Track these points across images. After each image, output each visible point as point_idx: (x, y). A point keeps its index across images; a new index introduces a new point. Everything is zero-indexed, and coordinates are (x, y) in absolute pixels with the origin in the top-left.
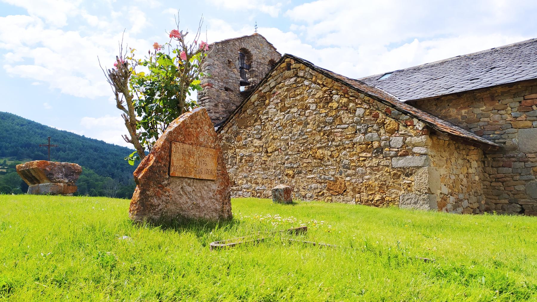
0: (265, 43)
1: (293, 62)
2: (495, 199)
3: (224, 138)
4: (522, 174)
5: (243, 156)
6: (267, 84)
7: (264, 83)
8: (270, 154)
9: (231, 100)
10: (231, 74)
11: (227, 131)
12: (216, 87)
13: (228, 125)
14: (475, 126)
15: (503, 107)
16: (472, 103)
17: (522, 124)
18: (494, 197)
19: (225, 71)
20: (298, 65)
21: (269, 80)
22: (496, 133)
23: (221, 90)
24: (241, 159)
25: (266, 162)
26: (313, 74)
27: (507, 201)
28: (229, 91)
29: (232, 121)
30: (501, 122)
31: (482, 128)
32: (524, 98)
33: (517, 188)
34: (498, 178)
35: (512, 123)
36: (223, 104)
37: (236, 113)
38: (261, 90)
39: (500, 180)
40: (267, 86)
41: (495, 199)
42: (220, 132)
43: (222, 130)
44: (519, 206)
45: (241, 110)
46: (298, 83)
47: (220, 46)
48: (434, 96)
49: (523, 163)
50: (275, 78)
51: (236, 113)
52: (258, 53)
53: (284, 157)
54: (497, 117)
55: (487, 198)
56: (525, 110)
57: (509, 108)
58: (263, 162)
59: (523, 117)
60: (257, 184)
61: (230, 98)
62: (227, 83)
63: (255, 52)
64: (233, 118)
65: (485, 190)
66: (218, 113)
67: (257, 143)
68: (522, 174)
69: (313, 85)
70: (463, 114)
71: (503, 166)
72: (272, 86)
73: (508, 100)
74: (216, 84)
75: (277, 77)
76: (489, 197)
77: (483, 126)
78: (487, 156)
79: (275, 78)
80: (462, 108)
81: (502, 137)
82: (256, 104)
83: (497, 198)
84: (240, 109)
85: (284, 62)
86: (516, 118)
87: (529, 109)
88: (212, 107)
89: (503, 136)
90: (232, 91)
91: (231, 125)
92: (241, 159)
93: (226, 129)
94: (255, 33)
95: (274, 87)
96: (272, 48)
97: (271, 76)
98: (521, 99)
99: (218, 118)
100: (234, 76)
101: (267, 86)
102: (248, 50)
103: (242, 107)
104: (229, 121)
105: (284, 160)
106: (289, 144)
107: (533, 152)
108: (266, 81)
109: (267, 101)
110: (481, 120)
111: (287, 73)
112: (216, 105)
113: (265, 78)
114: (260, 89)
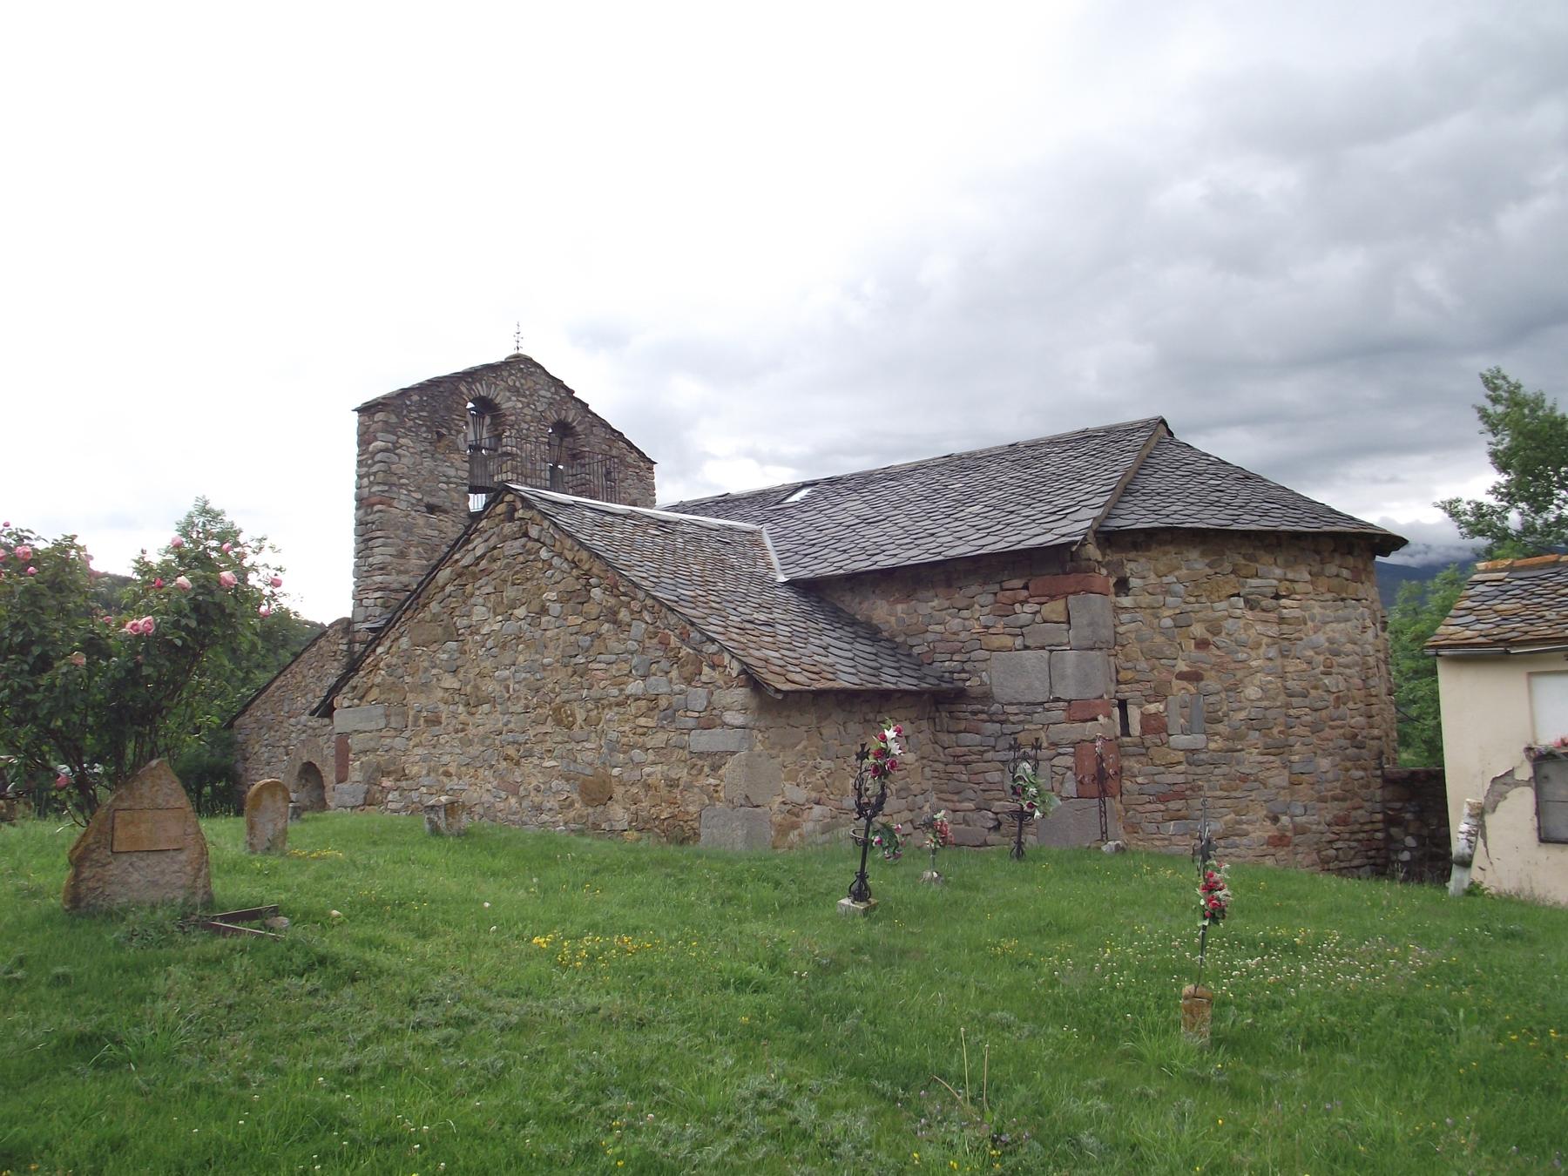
0: (542, 380)
1: (519, 505)
2: (952, 801)
3: (381, 665)
4: (997, 749)
5: (420, 711)
6: (470, 547)
7: (462, 546)
8: (474, 710)
9: (443, 535)
10: (446, 469)
11: (390, 647)
12: (403, 505)
13: (392, 635)
14: (920, 641)
15: (965, 602)
16: (915, 590)
17: (996, 642)
18: (950, 797)
19: (428, 463)
20: (529, 514)
21: (473, 540)
22: (955, 658)
23: (416, 511)
24: (416, 719)
25: (467, 727)
26: (557, 536)
27: (971, 805)
28: (438, 514)
29: (400, 627)
30: (963, 635)
31: (931, 645)
32: (1001, 587)
33: (989, 777)
34: (958, 757)
35: (981, 638)
36: (420, 549)
37: (407, 609)
38: (457, 561)
39: (961, 759)
40: (468, 551)
41: (952, 801)
42: (374, 651)
43: (378, 645)
44: (990, 814)
45: (418, 604)
46: (529, 552)
47: (415, 398)
48: (841, 572)
49: (999, 725)
50: (486, 536)
51: (407, 609)
52: (521, 406)
53: (501, 717)
54: (955, 624)
55: (939, 799)
56: (1002, 613)
57: (977, 606)
58: (461, 726)
59: (999, 627)
60: (447, 774)
61: (441, 531)
62: (431, 493)
63: (510, 404)
64: (400, 618)
65: (936, 781)
66: (406, 572)
67: (450, 682)
68: (997, 749)
69: (556, 561)
70: (899, 615)
71: (965, 731)
72: (478, 552)
73: (974, 589)
74: (402, 497)
75: (489, 533)
76: (941, 795)
77: (934, 642)
78: (940, 707)
79: (486, 536)
80: (897, 601)
81: (963, 669)
82: (449, 589)
83: (956, 798)
84: (415, 599)
85: (502, 502)
86: (987, 627)
87: (1008, 611)
88: (389, 559)
89: (967, 667)
90: (446, 512)
91: (398, 635)
92: (416, 719)
93: (387, 643)
94: (515, 352)
95: (482, 557)
96: (562, 391)
97: (476, 530)
98: (996, 588)
99: (406, 586)
100: (452, 472)
101: (468, 551)
102: (492, 400)
103: (419, 597)
104: (394, 626)
105: (500, 725)
106: (511, 690)
107: (1015, 701)
108: (468, 541)
109: (469, 588)
110: (930, 628)
111: (508, 528)
112: (402, 555)
113: (465, 533)
114: (457, 556)
